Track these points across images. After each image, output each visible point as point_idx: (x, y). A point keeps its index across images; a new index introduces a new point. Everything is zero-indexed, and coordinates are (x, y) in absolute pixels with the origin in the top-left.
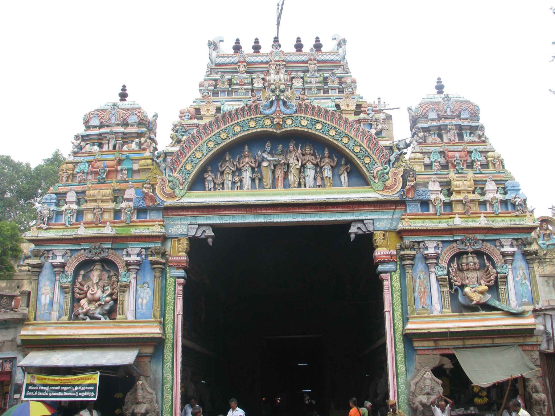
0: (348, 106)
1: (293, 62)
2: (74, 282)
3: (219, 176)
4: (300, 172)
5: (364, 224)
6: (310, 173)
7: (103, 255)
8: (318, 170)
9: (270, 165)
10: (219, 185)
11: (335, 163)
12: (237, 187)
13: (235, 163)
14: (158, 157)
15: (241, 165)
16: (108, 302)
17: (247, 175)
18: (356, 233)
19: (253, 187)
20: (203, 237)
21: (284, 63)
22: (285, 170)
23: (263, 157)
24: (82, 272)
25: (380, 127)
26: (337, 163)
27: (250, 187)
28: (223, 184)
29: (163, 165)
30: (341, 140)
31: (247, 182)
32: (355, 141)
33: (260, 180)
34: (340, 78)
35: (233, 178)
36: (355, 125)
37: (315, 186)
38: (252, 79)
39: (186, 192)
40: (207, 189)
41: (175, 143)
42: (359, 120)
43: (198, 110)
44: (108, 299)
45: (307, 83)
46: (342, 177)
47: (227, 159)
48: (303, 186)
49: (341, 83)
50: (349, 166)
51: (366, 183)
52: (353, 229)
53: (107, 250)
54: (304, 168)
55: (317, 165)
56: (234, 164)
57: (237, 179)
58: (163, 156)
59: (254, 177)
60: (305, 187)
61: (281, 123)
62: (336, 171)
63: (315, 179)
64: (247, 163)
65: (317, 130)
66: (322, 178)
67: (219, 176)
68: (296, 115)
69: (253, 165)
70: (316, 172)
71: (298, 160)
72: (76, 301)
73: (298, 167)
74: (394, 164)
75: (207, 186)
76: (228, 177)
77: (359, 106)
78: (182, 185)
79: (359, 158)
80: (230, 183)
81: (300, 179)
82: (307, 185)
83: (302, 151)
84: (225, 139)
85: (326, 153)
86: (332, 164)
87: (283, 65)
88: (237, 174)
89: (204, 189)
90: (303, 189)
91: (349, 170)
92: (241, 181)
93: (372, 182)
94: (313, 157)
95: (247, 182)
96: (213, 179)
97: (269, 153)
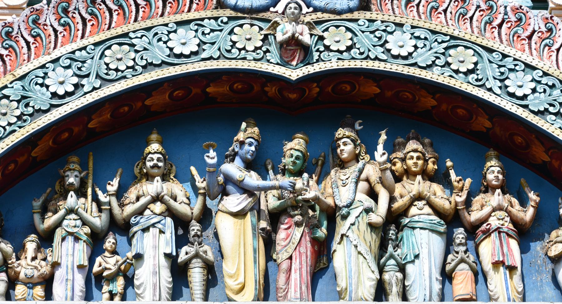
3: (31, 246)
4: (383, 247)
6: (423, 244)
10: (31, 284)
13: (102, 197)
15: (129, 209)
17: (155, 245)
23: (228, 179)
26: (538, 209)
28: (47, 282)
35: (92, 261)
54: (400, 228)
55: (452, 219)
59: (182, 257)
60: (405, 298)
61: (306, 39)
62: (537, 247)
63: (447, 276)
66: (479, 275)
67: (31, 246)
68: (368, 15)
69: (182, 208)
71: (373, 194)
76: (70, 254)
80: (80, 280)
81: (381, 270)
84: (68, 94)
85: (493, 171)
88: (109, 243)
94: (436, 188)
97: (249, 165)
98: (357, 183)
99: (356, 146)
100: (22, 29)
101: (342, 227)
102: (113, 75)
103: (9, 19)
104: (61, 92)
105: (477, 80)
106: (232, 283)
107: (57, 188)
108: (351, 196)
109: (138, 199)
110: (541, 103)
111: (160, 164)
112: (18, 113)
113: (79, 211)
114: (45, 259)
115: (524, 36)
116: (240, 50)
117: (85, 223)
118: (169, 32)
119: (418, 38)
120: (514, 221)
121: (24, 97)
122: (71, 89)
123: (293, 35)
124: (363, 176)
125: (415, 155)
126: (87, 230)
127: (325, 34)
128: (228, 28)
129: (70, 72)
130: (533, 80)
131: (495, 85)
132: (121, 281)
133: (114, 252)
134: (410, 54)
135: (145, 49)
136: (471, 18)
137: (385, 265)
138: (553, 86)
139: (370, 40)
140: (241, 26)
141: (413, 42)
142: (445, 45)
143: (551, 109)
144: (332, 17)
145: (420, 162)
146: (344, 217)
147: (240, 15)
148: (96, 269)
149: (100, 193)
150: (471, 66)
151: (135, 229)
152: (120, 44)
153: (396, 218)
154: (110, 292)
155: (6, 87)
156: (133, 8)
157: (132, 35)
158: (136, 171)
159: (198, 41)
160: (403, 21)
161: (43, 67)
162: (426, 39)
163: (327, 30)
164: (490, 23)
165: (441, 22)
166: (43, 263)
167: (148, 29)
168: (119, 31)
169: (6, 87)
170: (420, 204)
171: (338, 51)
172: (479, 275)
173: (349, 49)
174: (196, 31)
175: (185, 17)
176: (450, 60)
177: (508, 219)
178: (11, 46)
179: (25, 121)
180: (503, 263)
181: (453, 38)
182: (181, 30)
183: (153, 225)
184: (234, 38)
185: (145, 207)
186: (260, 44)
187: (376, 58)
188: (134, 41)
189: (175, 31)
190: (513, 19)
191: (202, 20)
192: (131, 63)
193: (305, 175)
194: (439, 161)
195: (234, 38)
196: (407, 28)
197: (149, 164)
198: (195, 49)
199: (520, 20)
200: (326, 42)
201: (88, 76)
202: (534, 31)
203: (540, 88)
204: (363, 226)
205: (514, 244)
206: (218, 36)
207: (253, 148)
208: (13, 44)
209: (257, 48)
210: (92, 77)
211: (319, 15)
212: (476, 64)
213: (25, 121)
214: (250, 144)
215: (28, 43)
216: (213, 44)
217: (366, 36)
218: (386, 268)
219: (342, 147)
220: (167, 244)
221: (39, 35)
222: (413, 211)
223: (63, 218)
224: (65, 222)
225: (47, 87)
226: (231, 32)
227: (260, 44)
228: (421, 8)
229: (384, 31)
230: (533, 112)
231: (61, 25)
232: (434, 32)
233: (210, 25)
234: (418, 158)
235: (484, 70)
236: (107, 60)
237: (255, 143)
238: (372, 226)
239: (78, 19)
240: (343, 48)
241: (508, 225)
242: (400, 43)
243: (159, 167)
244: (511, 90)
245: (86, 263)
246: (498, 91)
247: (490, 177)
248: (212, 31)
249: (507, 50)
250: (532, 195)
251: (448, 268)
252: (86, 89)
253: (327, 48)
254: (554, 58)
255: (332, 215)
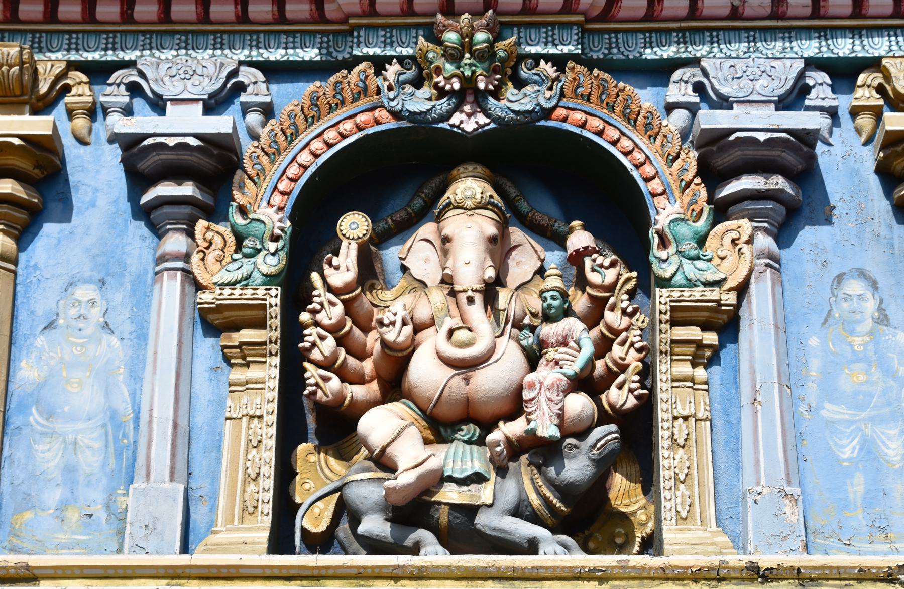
2: (295, 288)
7: (516, 101)
16: (581, 435)
24: (354, 225)
44: (579, 404)
53: (548, 69)
72: (314, 423)
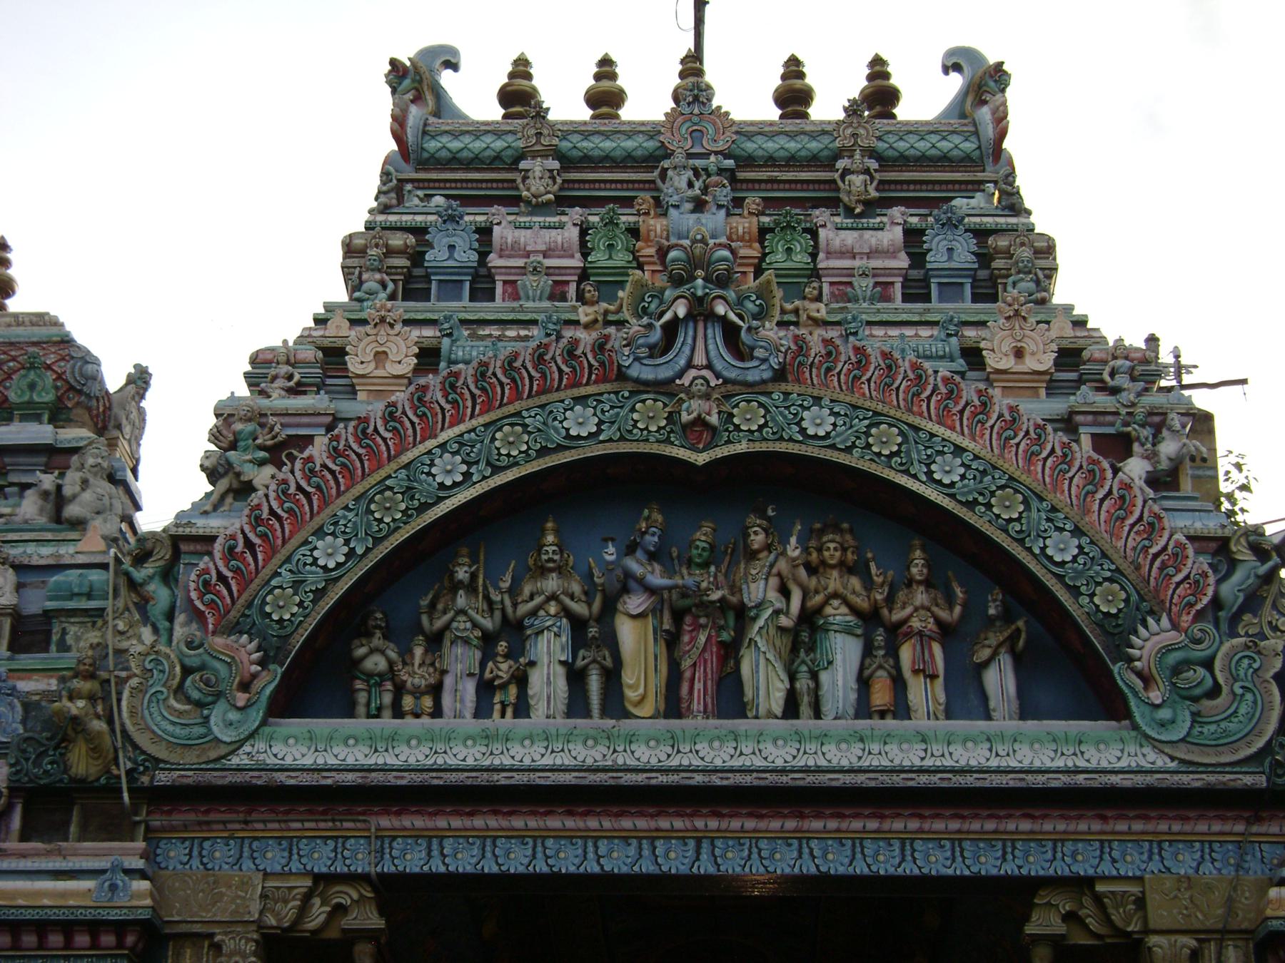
0: (1019, 353)
1: (771, 161)
3: (418, 651)
4: (794, 650)
5: (1098, 899)
8: (879, 638)
9: (656, 611)
10: (417, 693)
11: (958, 609)
12: (504, 707)
13: (496, 597)
14: (141, 557)
15: (523, 609)
17: (549, 652)
18: (1056, 942)
19: (577, 705)
20: (333, 934)
21: (730, 163)
22: (725, 636)
23: (628, 575)
25: (1168, 448)
27: (562, 707)
28: (436, 690)
29: (160, 594)
30: (989, 506)
31: (547, 682)
32: (1054, 509)
33: (612, 677)
34: (981, 234)
35: (483, 665)
36: (1055, 439)
37: (863, 709)
38: (583, 233)
39: (264, 723)
40: (361, 709)
41: (222, 498)
42: (1072, 413)
43: (334, 355)
45: (829, 254)
46: (991, 678)
47: (462, 574)
48: (805, 709)
49: (984, 259)
50: (1020, 624)
51: (1108, 703)
52: (1045, 921)
55: (869, 619)
56: (490, 603)
57: (505, 668)
58: (165, 553)
59: (580, 663)
61: (714, 419)
63: (864, 683)
64: (553, 597)
65: (877, 454)
67: (418, 651)
68: (784, 387)
69: (579, 608)
70: (868, 651)
71: (785, 592)
73: (784, 621)
74: (1235, 619)
75: (362, 697)
76: (461, 660)
77: (1069, 356)
78: (245, 686)
79: (1075, 591)
80: (470, 687)
81: (792, 678)
82: (827, 707)
83: (806, 550)
84: (455, 485)
86: (944, 614)
87: (721, 171)
88: (502, 646)
89: (350, 712)
90: (805, 723)
91: (1021, 643)
92: (521, 680)
93: (1133, 703)
94: (855, 582)
95: (547, 682)
96: (391, 664)
97: (652, 557)
98: (766, 579)
99: (767, 535)
100: (407, 409)
101: (753, 632)
102: (505, 461)
103: (393, 398)
104: (448, 483)
105: (901, 464)
106: (631, 695)
107: (446, 584)
108: (761, 595)
109: (532, 597)
110: (970, 492)
111: (556, 557)
112: (403, 506)
113: (468, 613)
114: (433, 664)
115: (954, 410)
116: (642, 430)
117: (475, 625)
118: (566, 410)
119: (837, 414)
120: (938, 622)
121: (409, 488)
122: (459, 478)
123: (699, 415)
124: (775, 571)
125: (832, 545)
126: (478, 633)
127: (735, 411)
128: (629, 404)
129: (458, 458)
130: (963, 465)
131: (918, 469)
132: (513, 690)
133: (507, 656)
134: (828, 434)
135: (539, 430)
136: (898, 389)
137: (796, 672)
138: (984, 473)
139: (785, 417)
140: (643, 401)
141: (832, 419)
142: (866, 422)
143: (981, 499)
144: (744, 389)
145: (838, 554)
146: (754, 619)
147: (642, 388)
148: (487, 675)
149: (491, 590)
150: (895, 448)
151: (529, 632)
152: (512, 425)
153: (810, 620)
154: (502, 702)
155: (389, 477)
156: (527, 381)
157: (525, 414)
158: (531, 562)
159: (596, 420)
160: (822, 393)
161: (429, 452)
162: (846, 415)
163: (737, 406)
164: (919, 395)
165: (864, 394)
166: (431, 670)
167: (542, 407)
168: (511, 409)
169: (389, 477)
170: (836, 603)
171: (749, 431)
172: (899, 684)
173: (761, 427)
174: (595, 408)
175: (583, 391)
176: (871, 440)
177: (931, 620)
178: (395, 428)
179: (411, 516)
180: (923, 671)
181: (876, 413)
182: (578, 408)
183: (548, 628)
184: (635, 416)
185: (539, 607)
186: (663, 423)
187: (791, 440)
188: (527, 421)
189: (572, 409)
190: (944, 390)
191: (601, 394)
192: (524, 448)
193: (713, 569)
194: (857, 550)
195: (635, 416)
196: (826, 401)
197: (545, 557)
198: (594, 429)
199: (951, 392)
200: (736, 421)
201: (477, 463)
202: (967, 404)
203: (970, 475)
204: (772, 631)
205: (937, 649)
206: (618, 414)
207: (656, 539)
208: (398, 425)
209: (660, 428)
210: (482, 465)
211: (729, 387)
212: (900, 445)
213: (411, 516)
214: (653, 534)
215: (412, 423)
216: (613, 423)
217: (781, 413)
218: (799, 676)
219: (753, 537)
220: (563, 649)
221: (424, 414)
222: (828, 610)
223: (453, 620)
224: (455, 625)
225: (434, 476)
226: (633, 410)
227: (663, 423)
228: (842, 377)
229: (801, 406)
230: (960, 502)
231: (448, 402)
232: (855, 407)
233: (610, 400)
234: (835, 549)
235: (908, 453)
236: (497, 444)
237: (659, 532)
238: (782, 630)
239: (467, 396)
240: (755, 427)
241: (931, 625)
242: (818, 421)
243: (554, 561)
244: (936, 476)
245: (477, 671)
246: (924, 478)
247: (914, 570)
248: (612, 407)
249: (936, 428)
250: (959, 592)
251: (867, 673)
252: (475, 478)
253: (737, 428)
254: (987, 436)
255: (743, 615)
